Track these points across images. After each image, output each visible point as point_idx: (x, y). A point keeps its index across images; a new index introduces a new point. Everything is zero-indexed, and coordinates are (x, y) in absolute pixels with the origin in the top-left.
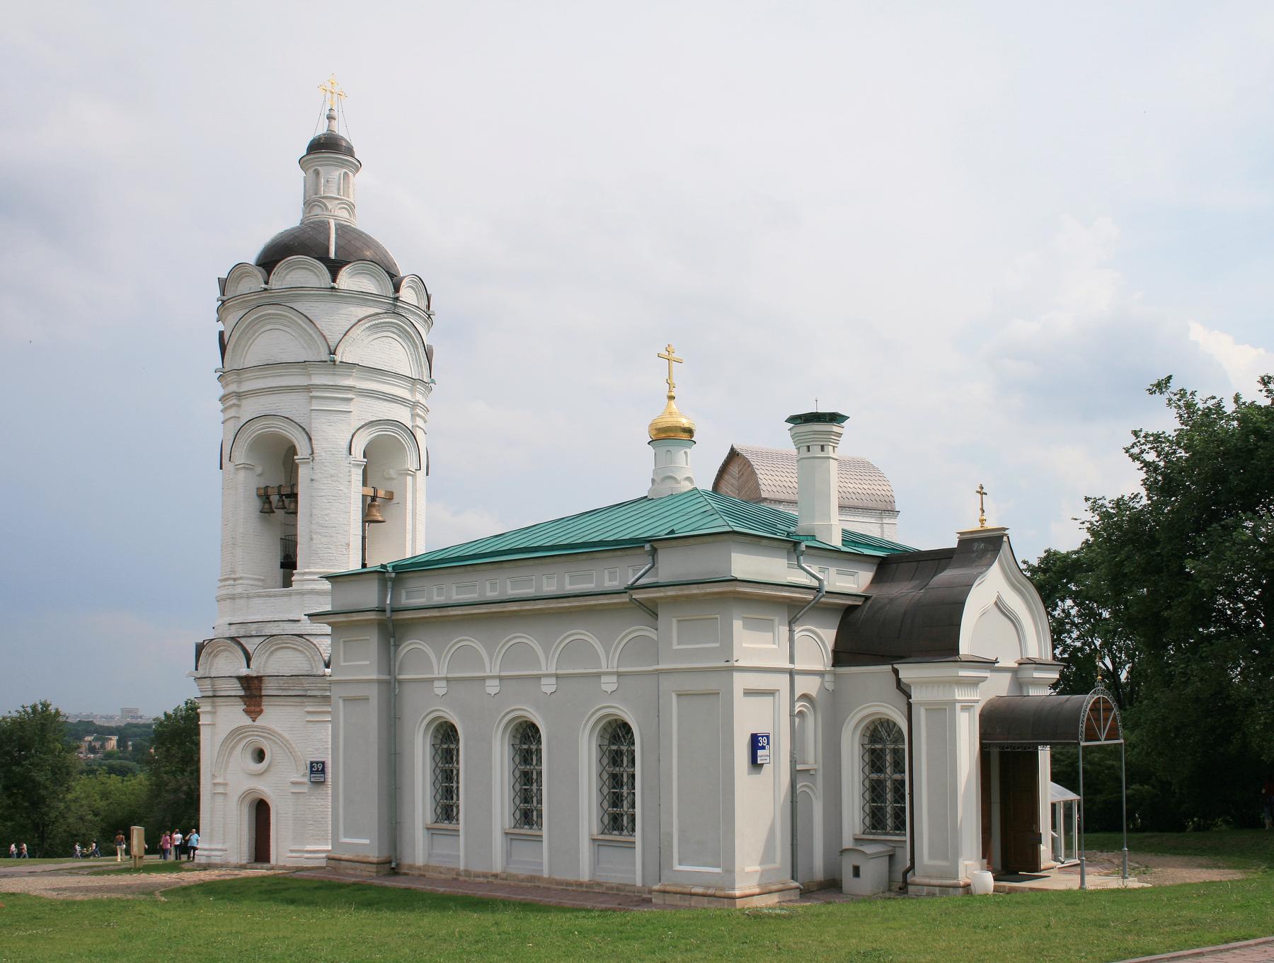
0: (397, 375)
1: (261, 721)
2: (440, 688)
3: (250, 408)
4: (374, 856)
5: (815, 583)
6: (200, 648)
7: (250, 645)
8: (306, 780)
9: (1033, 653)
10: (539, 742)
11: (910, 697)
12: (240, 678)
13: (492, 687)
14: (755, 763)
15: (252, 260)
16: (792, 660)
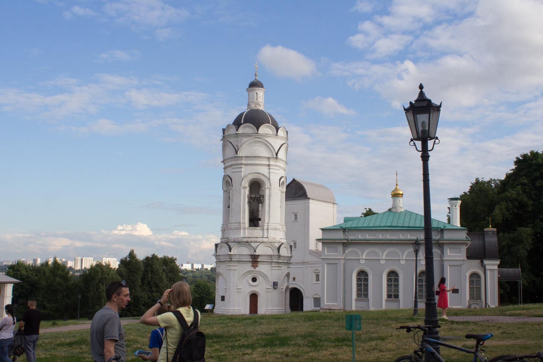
1: (257, 269)
2: (362, 262)
4: (341, 307)
7: (231, 245)
8: (272, 287)
12: (251, 255)
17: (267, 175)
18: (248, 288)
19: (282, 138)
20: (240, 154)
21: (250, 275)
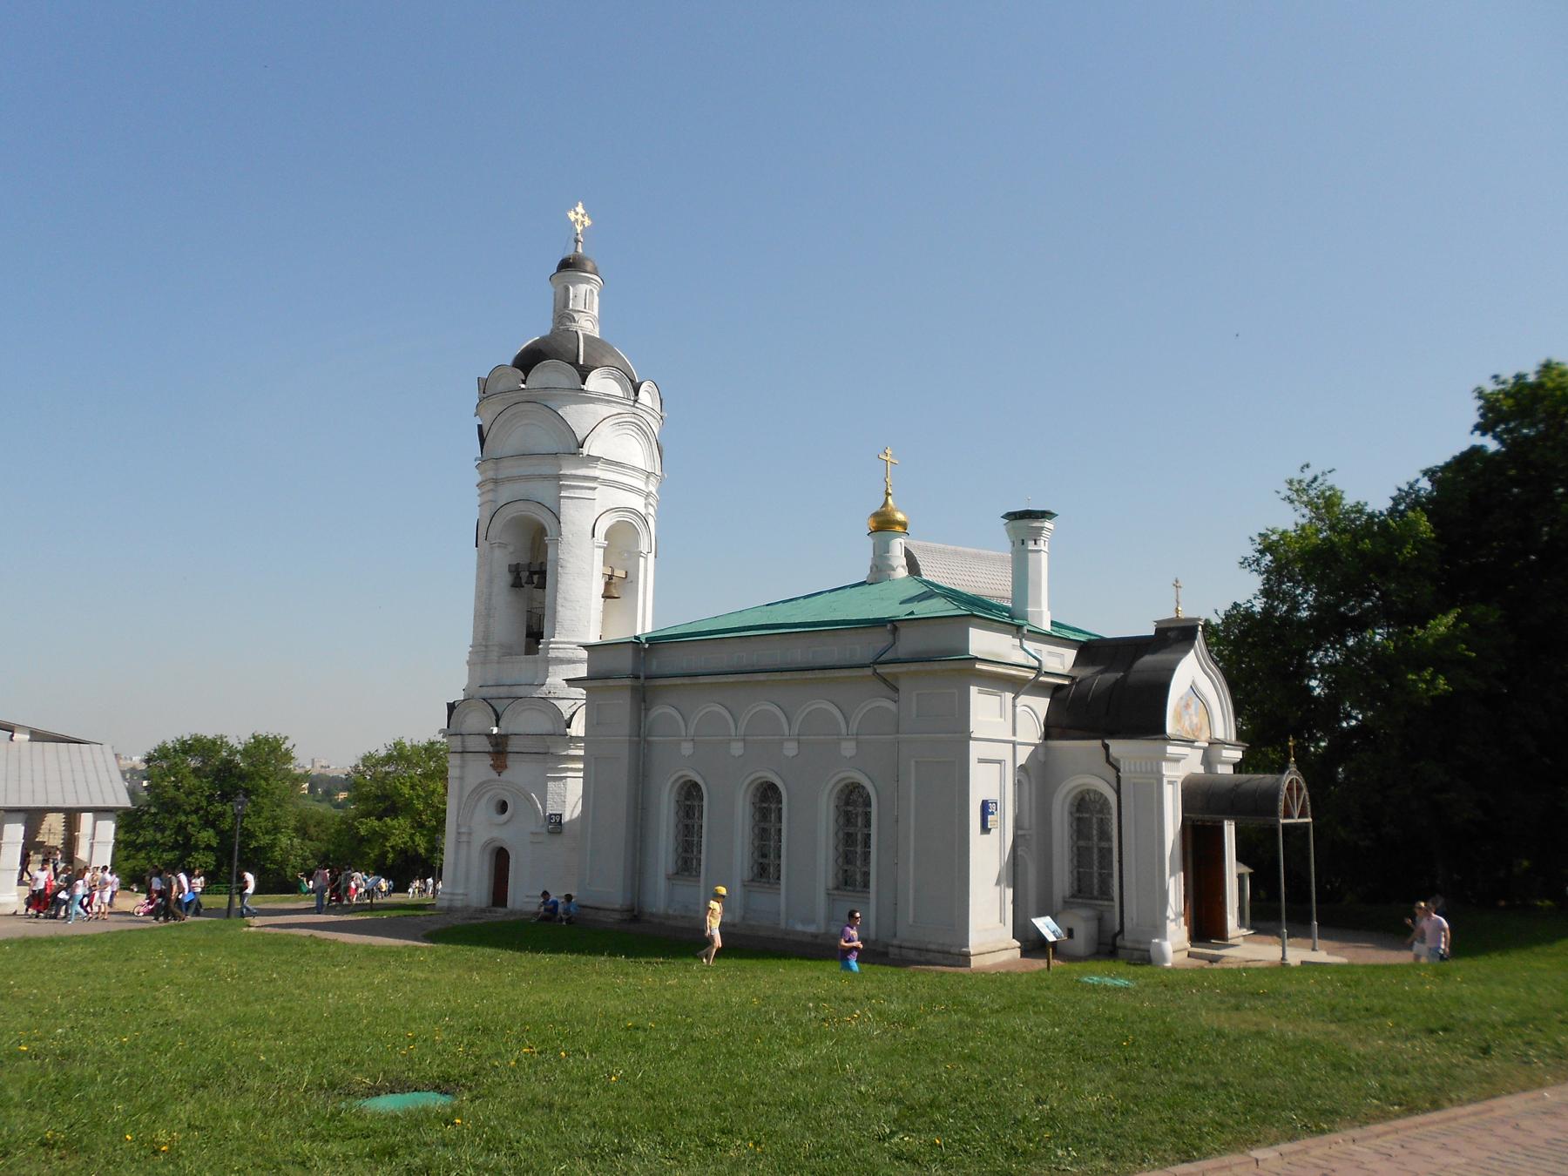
0: (634, 468)
1: (506, 775)
3: (506, 493)
5: (1036, 664)
6: (451, 707)
9: (1219, 734)
10: (780, 802)
11: (1118, 770)
13: (737, 749)
14: (985, 829)
15: (509, 362)
16: (1014, 734)
19: (606, 399)
21: (487, 797)
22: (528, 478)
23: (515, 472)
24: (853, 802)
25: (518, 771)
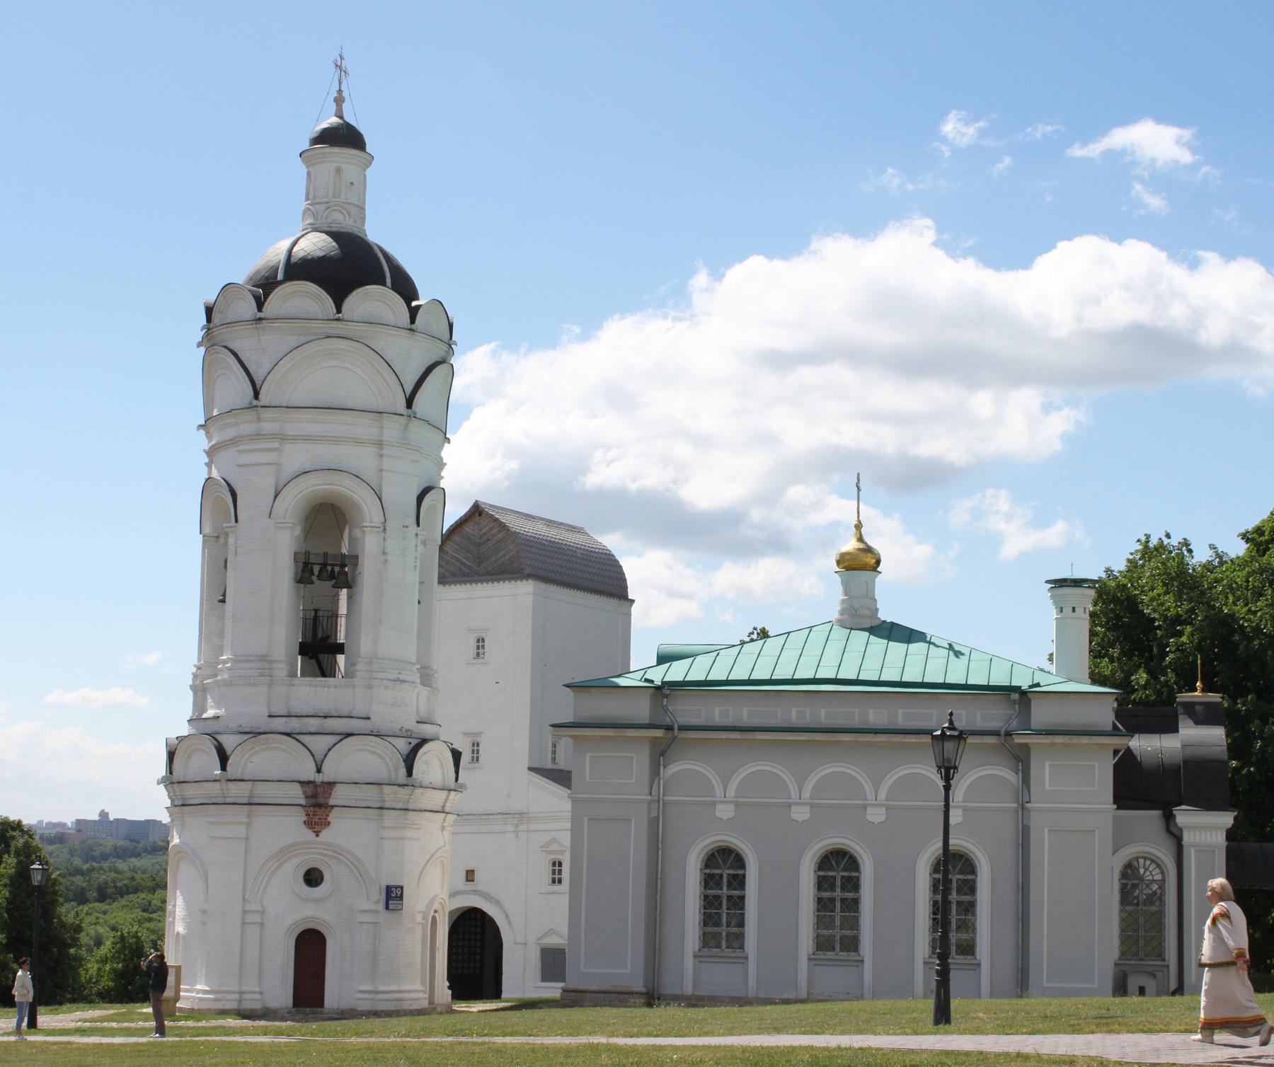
1: (326, 834)
3: (296, 457)
17: (370, 474)
18: (290, 909)
20: (265, 398)
21: (296, 861)
22: (335, 440)
23: (316, 429)
24: (953, 872)
25: (345, 830)
